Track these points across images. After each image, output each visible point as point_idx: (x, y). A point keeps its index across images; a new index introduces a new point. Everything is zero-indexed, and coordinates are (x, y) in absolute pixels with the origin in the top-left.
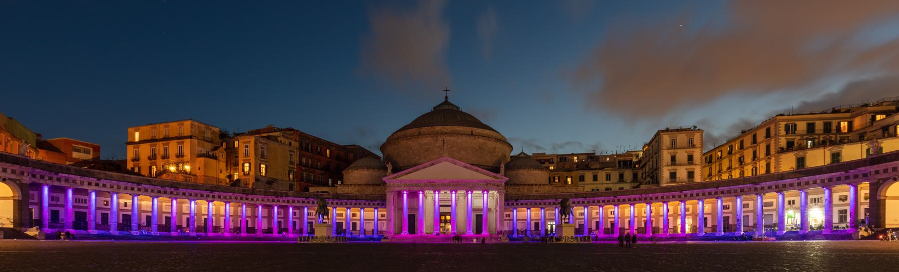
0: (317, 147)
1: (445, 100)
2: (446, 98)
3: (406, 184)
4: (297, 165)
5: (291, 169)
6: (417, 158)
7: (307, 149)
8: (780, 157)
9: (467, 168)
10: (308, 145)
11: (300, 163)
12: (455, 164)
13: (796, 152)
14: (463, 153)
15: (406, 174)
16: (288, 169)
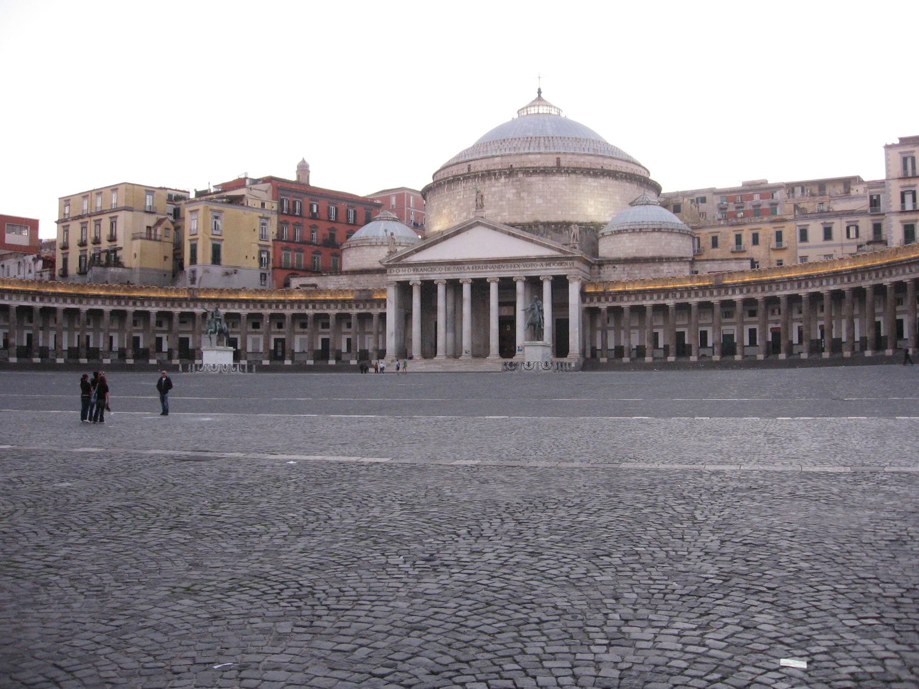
0: (311, 206)
1: (537, 95)
2: (539, 92)
3: (417, 270)
4: (273, 240)
5: (263, 248)
7: (291, 213)
9: (513, 235)
10: (294, 203)
11: (279, 238)
12: (495, 229)
14: (539, 201)
15: (417, 251)
16: (258, 248)
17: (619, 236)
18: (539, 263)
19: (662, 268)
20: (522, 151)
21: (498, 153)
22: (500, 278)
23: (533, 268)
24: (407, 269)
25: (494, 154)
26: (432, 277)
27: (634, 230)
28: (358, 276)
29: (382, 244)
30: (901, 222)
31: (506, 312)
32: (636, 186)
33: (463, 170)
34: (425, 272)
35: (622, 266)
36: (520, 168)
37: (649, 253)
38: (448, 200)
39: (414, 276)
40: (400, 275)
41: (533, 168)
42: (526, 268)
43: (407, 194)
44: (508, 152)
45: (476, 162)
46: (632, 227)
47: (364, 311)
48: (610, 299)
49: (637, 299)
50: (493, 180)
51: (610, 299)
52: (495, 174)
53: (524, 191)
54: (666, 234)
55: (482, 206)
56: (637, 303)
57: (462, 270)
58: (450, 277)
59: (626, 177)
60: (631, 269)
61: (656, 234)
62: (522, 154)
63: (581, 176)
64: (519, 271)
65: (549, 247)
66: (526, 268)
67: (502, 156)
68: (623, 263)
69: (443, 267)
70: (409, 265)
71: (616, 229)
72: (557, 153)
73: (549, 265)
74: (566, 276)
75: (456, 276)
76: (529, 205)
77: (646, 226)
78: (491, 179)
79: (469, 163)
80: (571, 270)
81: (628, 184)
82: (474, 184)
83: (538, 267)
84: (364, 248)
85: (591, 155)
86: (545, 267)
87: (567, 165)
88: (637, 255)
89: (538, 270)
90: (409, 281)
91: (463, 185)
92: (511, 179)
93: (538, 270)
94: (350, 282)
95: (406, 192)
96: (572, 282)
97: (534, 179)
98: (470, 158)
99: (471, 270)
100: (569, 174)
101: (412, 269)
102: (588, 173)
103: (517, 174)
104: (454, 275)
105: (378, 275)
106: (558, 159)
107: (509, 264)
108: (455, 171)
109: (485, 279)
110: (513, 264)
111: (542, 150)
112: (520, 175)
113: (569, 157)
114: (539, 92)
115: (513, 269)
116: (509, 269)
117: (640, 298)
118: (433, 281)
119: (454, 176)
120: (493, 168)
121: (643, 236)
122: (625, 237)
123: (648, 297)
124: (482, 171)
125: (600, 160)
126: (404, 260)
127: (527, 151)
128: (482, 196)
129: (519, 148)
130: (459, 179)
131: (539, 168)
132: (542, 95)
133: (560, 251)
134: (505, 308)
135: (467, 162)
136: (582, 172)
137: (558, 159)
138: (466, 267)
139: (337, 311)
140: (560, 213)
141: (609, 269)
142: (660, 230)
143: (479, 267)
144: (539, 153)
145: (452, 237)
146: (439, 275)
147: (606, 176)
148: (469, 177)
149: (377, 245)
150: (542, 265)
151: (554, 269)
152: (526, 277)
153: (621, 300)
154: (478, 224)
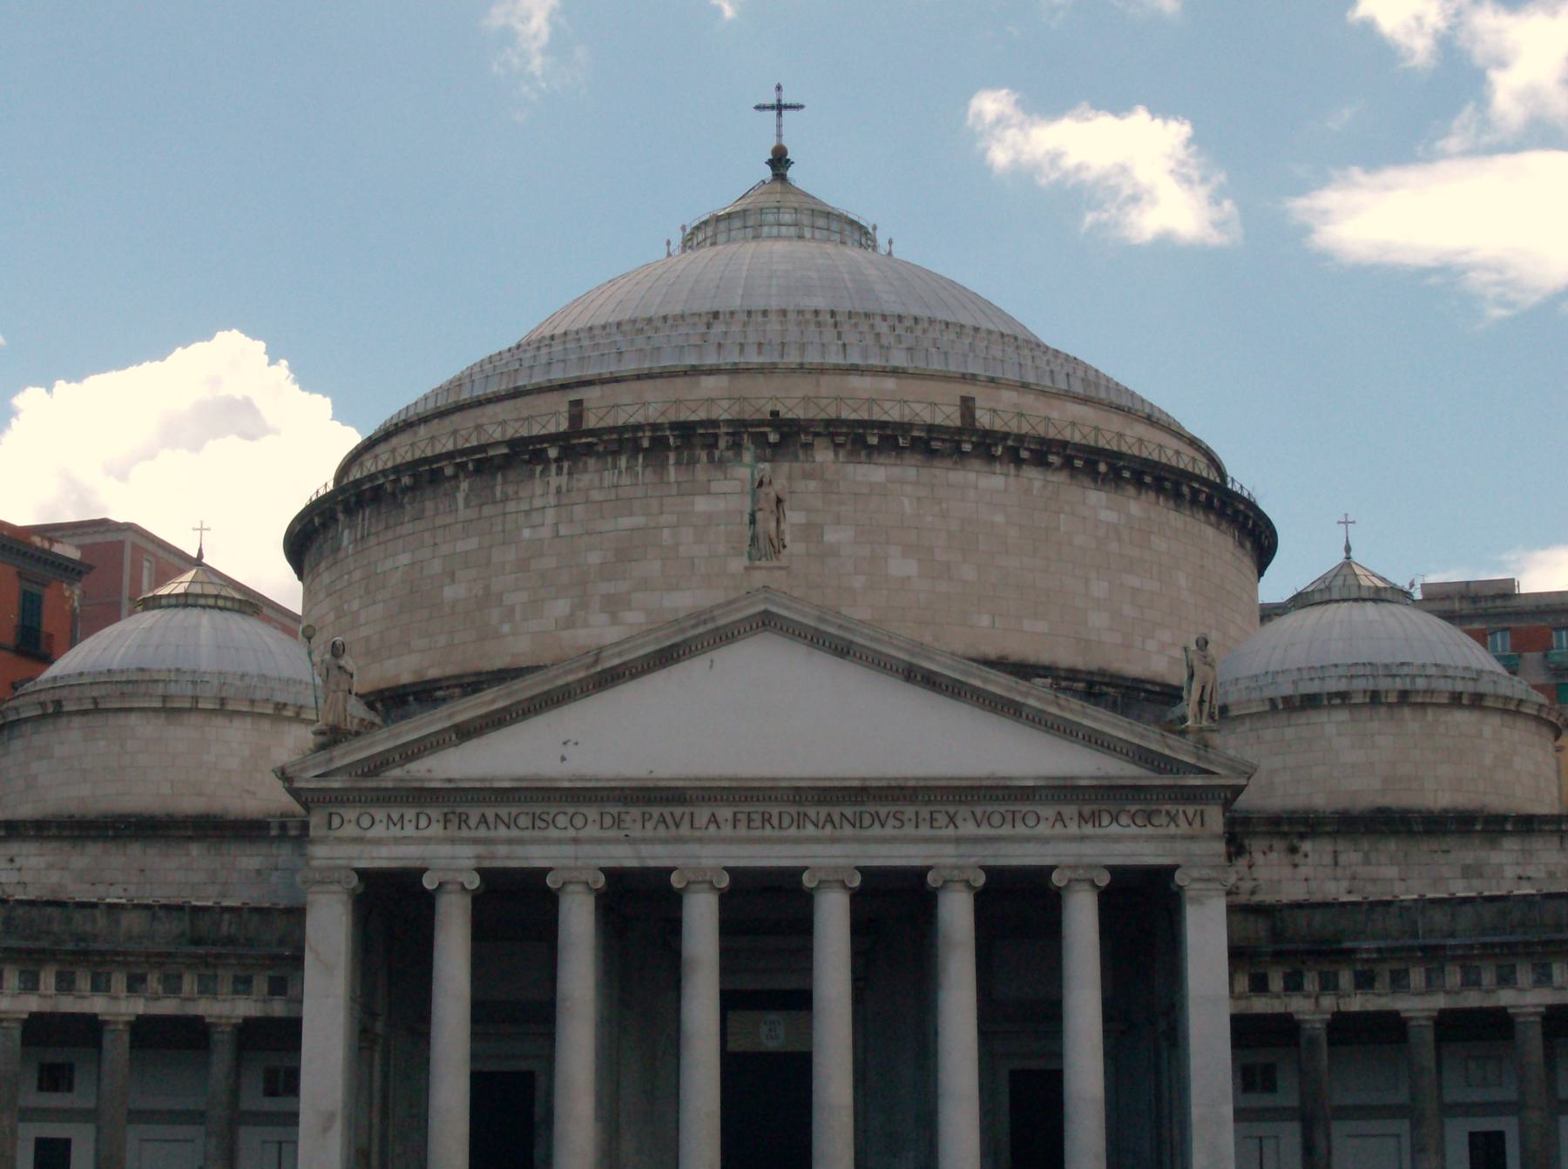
1: (767, 173)
2: (779, 161)
6: (561, 607)
12: (843, 650)
14: (901, 567)
15: (465, 732)
17: (1302, 718)
18: (1048, 812)
19: (1496, 857)
20: (813, 357)
21: (711, 360)
22: (865, 872)
23: (1021, 829)
24: (410, 813)
25: (691, 360)
26: (534, 856)
27: (1375, 698)
28: (94, 849)
29: (223, 709)
31: (770, 1034)
32: (1230, 540)
33: (550, 418)
34: (502, 832)
35: (1327, 846)
36: (829, 423)
37: (1438, 797)
38: (472, 543)
39: (445, 850)
40: (379, 842)
41: (883, 425)
42: (985, 830)
43: (135, 547)
44: (753, 358)
45: (608, 389)
46: (1359, 684)
47: (167, 1007)
48: (1346, 979)
49: (1471, 981)
50: (701, 472)
51: (1346, 979)
52: (711, 444)
53: (838, 521)
54: (1494, 721)
55: (777, 546)
56: (1473, 1000)
57: (685, 830)
58: (625, 857)
59: (1209, 498)
60: (1367, 861)
61: (1461, 717)
62: (821, 370)
63: (1061, 477)
64: (958, 840)
65: (1095, 740)
66: (985, 830)
67: (735, 371)
68: (1334, 835)
69: (592, 812)
70: (422, 796)
71: (1288, 690)
72: (966, 378)
73: (1094, 818)
74: (1168, 872)
75: (655, 855)
76: (858, 582)
77: (1421, 684)
78: (693, 462)
79: (574, 395)
80: (1197, 848)
81: (1210, 532)
82: (609, 477)
83: (1043, 829)
84: (133, 719)
85: (1085, 400)
86: (1073, 829)
87: (1013, 427)
88: (1389, 801)
89: (1045, 840)
90: (423, 871)
91: (554, 480)
92: (785, 467)
93: (1045, 840)
94: (54, 877)
95: (130, 538)
96: (1198, 901)
97: (876, 473)
98: (574, 373)
99: (727, 831)
100: (1019, 462)
101: (435, 813)
102: (1090, 470)
103: (808, 447)
104: (645, 850)
105: (195, 849)
106: (967, 405)
107: (909, 811)
108: (499, 425)
109: (797, 872)
110: (925, 812)
111: (899, 359)
112: (823, 455)
113: (1008, 397)
114: (779, 161)
115: (925, 830)
116: (909, 830)
117: (1488, 977)
118: (544, 872)
119: (513, 443)
120: (701, 415)
121: (1411, 721)
122: (1332, 723)
123: (1524, 975)
124: (655, 427)
125: (1115, 423)
126: (397, 772)
127: (834, 358)
128: (779, 501)
129: (802, 347)
130: (538, 457)
131: (905, 427)
132: (791, 173)
133: (1143, 757)
134: (773, 1016)
135: (564, 387)
136: (1068, 464)
137: (967, 405)
138: (703, 814)
139: (33, 1004)
140: (985, 621)
141: (1274, 856)
142: (1477, 702)
143: (766, 820)
144: (895, 372)
145: (633, 676)
146: (569, 850)
147: (1148, 487)
148: (589, 450)
149: (194, 710)
150: (1060, 817)
151: (1118, 839)
152: (988, 870)
153: (1399, 982)
154: (767, 622)
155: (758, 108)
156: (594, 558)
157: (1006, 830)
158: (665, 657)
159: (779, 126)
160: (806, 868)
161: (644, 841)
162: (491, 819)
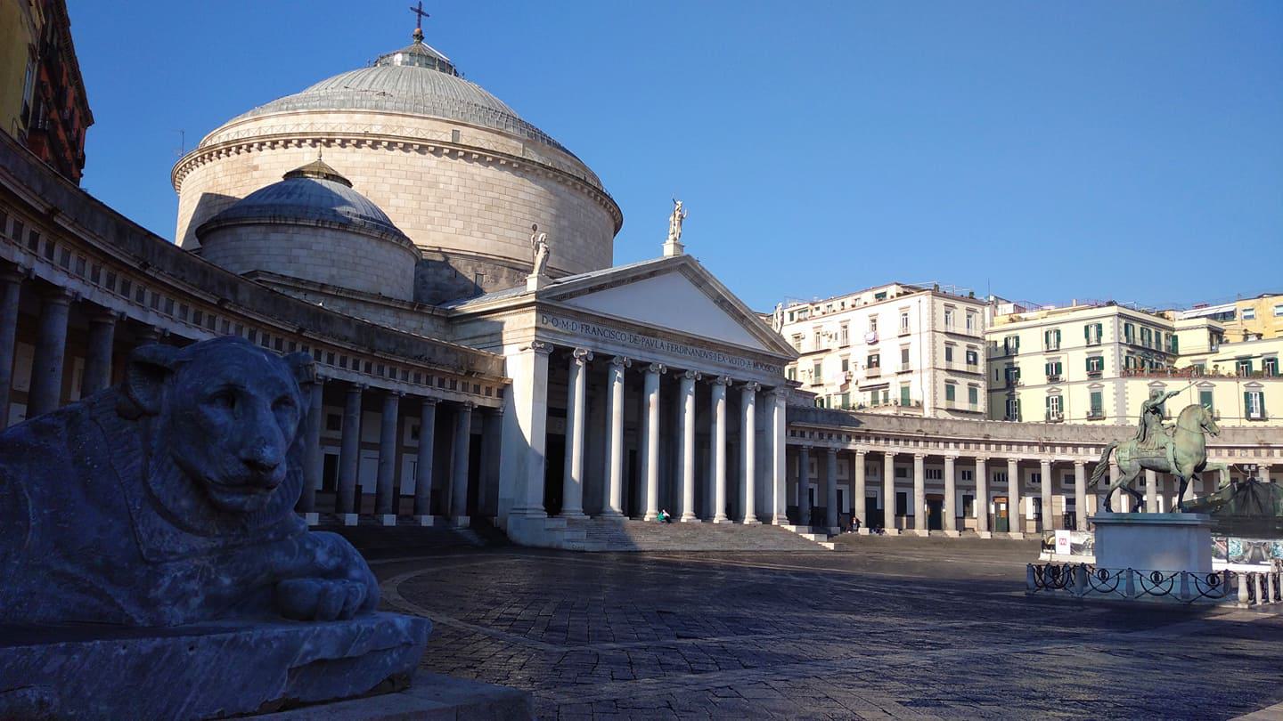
8: (1126, 385)
12: (699, 286)
13: (1150, 381)
14: (580, 241)
24: (570, 322)
26: (610, 349)
30: (946, 381)
66: (732, 365)
70: (579, 315)
138: (659, 341)
155: (412, 8)
156: (476, 206)
157: (736, 366)
158: (652, 274)
159: (419, 21)
160: (686, 370)
161: (644, 350)
162: (596, 330)
